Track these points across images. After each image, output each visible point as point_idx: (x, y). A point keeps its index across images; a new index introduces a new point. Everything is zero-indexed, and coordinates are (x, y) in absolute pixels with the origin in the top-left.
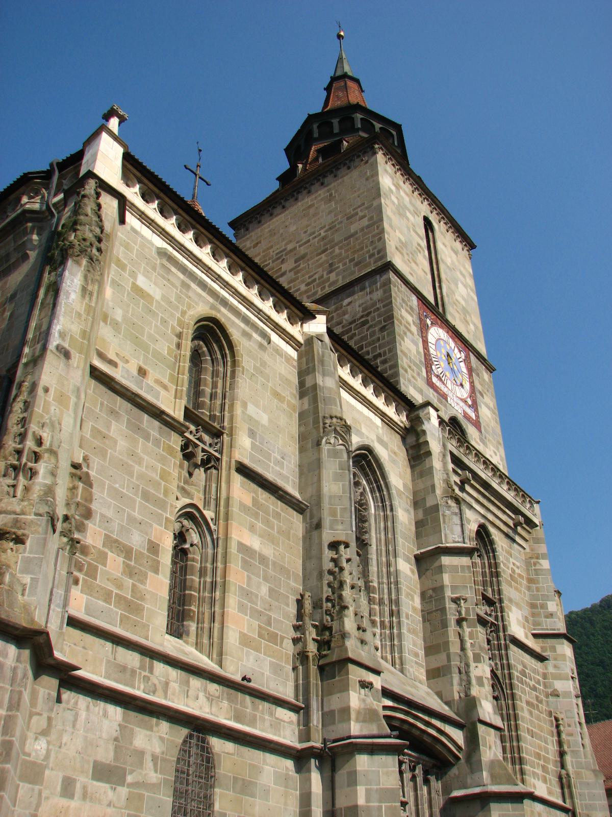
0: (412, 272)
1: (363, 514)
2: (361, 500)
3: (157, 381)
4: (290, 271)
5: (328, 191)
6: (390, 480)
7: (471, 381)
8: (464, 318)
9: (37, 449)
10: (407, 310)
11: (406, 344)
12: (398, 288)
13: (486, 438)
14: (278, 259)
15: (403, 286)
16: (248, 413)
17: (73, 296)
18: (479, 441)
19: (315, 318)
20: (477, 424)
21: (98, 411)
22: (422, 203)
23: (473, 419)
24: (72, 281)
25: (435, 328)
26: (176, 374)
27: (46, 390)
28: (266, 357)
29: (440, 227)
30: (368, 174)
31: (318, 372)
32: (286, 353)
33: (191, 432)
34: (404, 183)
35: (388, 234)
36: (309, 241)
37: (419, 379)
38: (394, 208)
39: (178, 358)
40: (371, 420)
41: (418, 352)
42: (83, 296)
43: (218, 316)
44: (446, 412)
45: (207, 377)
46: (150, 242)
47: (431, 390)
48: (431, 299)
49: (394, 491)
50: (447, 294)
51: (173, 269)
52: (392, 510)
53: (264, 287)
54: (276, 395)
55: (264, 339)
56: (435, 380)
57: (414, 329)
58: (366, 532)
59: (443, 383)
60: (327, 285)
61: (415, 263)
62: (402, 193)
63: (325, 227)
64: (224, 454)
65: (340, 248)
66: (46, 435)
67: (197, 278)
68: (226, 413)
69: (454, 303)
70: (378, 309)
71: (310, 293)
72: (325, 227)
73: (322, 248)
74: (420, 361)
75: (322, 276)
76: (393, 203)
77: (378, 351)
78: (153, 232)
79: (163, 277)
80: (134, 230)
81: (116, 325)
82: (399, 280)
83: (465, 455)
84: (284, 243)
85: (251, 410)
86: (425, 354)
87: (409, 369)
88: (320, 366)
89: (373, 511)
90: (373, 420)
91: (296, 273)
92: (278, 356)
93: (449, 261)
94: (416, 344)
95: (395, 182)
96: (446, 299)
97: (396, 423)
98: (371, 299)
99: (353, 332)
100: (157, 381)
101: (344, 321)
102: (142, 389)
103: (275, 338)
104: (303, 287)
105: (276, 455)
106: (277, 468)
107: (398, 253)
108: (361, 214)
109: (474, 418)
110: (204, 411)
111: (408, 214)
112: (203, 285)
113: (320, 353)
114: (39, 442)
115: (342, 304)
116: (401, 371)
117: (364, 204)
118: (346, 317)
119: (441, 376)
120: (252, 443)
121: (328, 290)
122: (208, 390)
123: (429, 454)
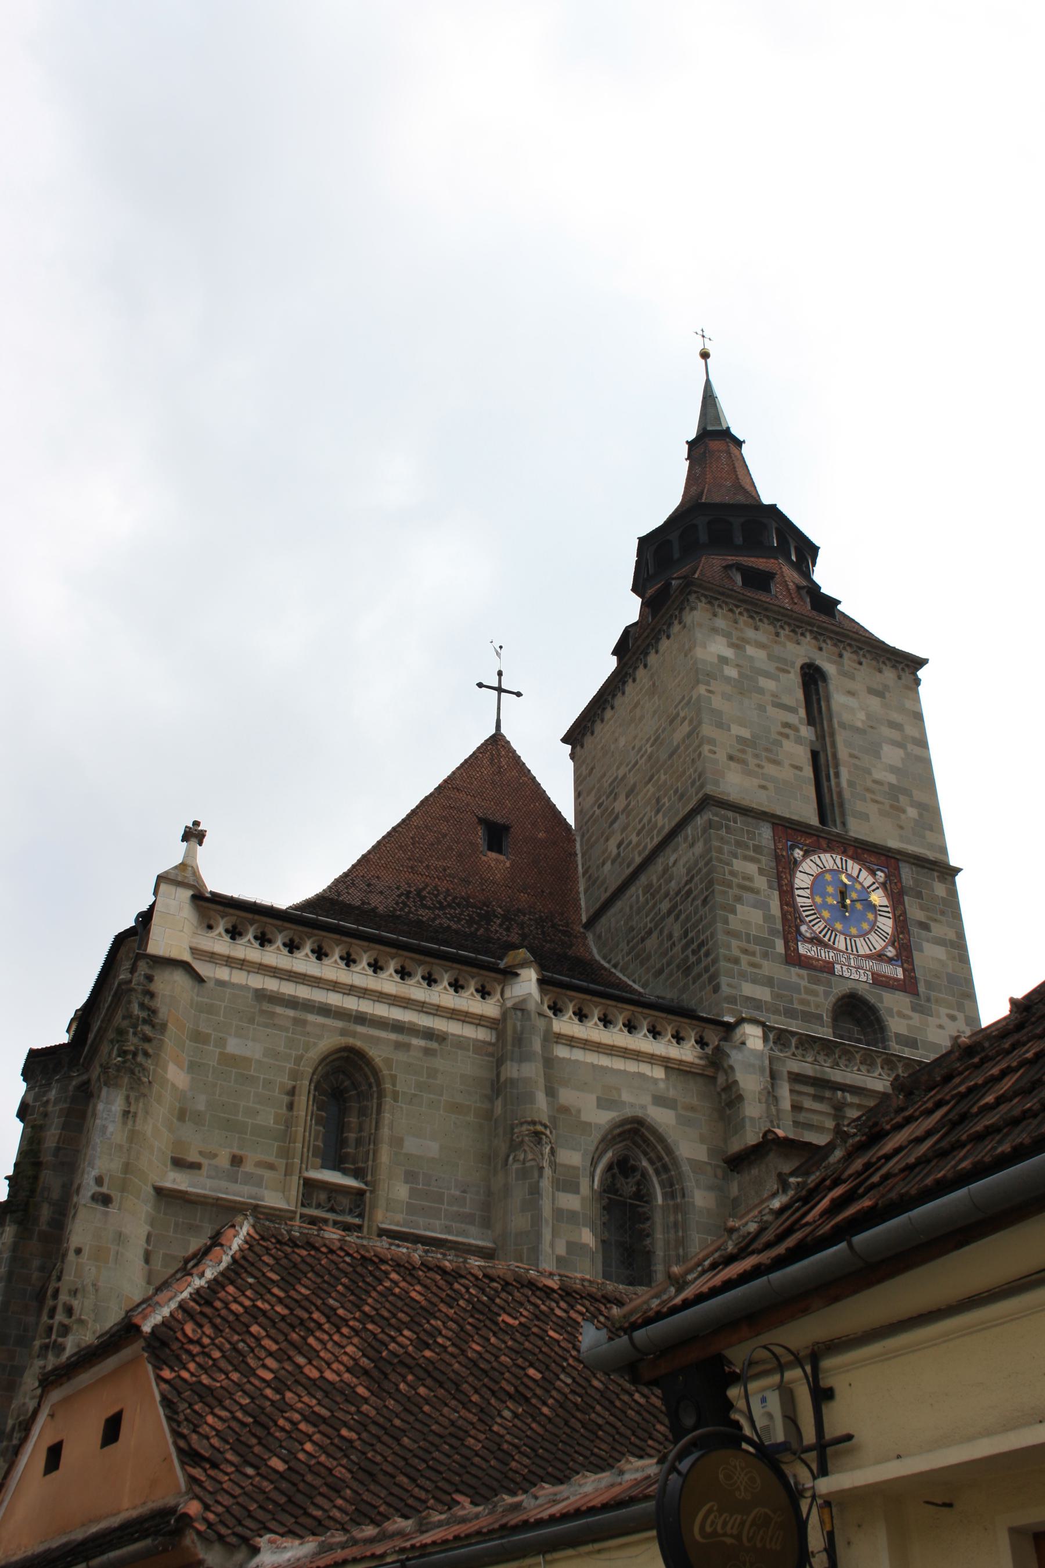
0: (764, 783)
1: (641, 1210)
2: (639, 1190)
3: (259, 1164)
4: (622, 813)
5: (652, 677)
6: (677, 1153)
7: (898, 913)
8: (892, 806)
9: (66, 1321)
10: (746, 858)
11: (739, 916)
12: (728, 828)
13: (928, 1000)
14: (611, 793)
15: (739, 818)
16: (404, 1151)
17: (111, 1128)
18: (909, 1013)
19: (517, 975)
20: (909, 985)
21: (171, 1234)
22: (798, 644)
23: (897, 980)
24: (110, 1111)
25: (815, 858)
26: (287, 1145)
27: (78, 1251)
28: (439, 1063)
29: (840, 664)
30: (687, 647)
31: (512, 1060)
32: (476, 1040)
33: (319, 1206)
34: (756, 629)
35: (712, 742)
36: (636, 763)
37: (765, 963)
38: (728, 689)
39: (289, 1123)
40: (641, 1076)
41: (768, 918)
42: (125, 1123)
43: (351, 1041)
44: (827, 994)
45: (353, 1120)
46: (246, 987)
47: (795, 970)
48: (807, 812)
49: (686, 1168)
50: (851, 784)
51: (279, 1010)
52: (684, 1196)
53: (432, 964)
54: (456, 1108)
55: (431, 1040)
56: (803, 949)
57: (761, 882)
58: (648, 1235)
59: (826, 945)
60: (655, 832)
61: (776, 762)
62: (750, 650)
63: (650, 738)
64: (366, 1218)
65: (665, 774)
66: (76, 1303)
67: (314, 1007)
68: (370, 1163)
69: (868, 790)
70: (700, 870)
71: (641, 848)
72: (650, 738)
73: (649, 774)
74: (773, 932)
75: (650, 821)
76: (728, 680)
77: (702, 937)
78: (249, 972)
79: (266, 1026)
80: (221, 983)
81: (198, 1118)
82: (730, 814)
83: (835, 1065)
84: (615, 768)
85: (411, 1145)
86: (784, 915)
87: (744, 959)
88: (516, 1049)
89: (660, 1201)
90: (649, 1073)
91: (627, 817)
92: (460, 1052)
93: (859, 719)
94: (763, 906)
95: (735, 641)
96: (847, 794)
97: (692, 1063)
98: (693, 854)
99: (679, 908)
100: (259, 1164)
101: (672, 893)
102: (236, 1182)
103: (453, 1028)
104: (635, 839)
105: (452, 1191)
106: (455, 1209)
107: (733, 764)
108: (682, 714)
109: (901, 976)
110: (347, 1165)
111: (763, 682)
112: (325, 1010)
113: (519, 1028)
114: (69, 1311)
115: (668, 864)
116: (723, 964)
117: (683, 698)
118: (673, 883)
119: (821, 935)
120: (411, 1189)
121: (656, 841)
122: (352, 1136)
123: (740, 1098)
